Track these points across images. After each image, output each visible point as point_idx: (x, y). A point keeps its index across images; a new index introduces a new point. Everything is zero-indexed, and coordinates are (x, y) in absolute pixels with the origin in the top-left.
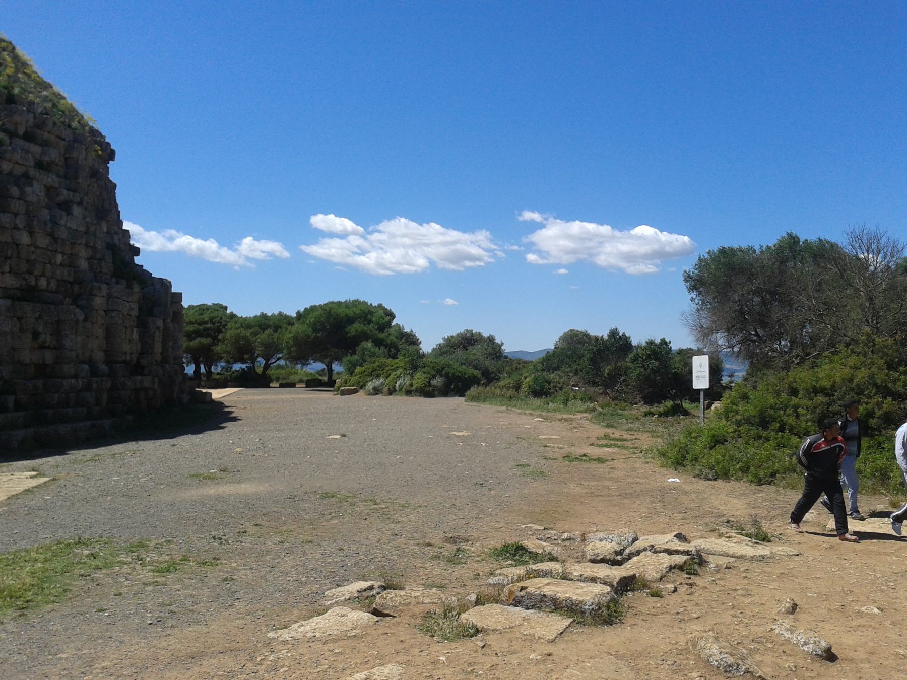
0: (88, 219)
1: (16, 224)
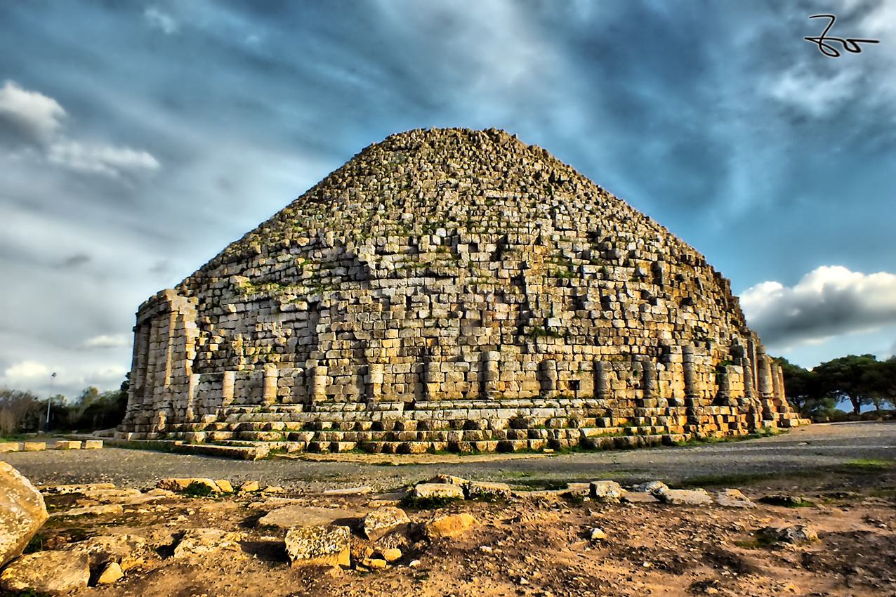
0: (668, 307)
1: (614, 317)
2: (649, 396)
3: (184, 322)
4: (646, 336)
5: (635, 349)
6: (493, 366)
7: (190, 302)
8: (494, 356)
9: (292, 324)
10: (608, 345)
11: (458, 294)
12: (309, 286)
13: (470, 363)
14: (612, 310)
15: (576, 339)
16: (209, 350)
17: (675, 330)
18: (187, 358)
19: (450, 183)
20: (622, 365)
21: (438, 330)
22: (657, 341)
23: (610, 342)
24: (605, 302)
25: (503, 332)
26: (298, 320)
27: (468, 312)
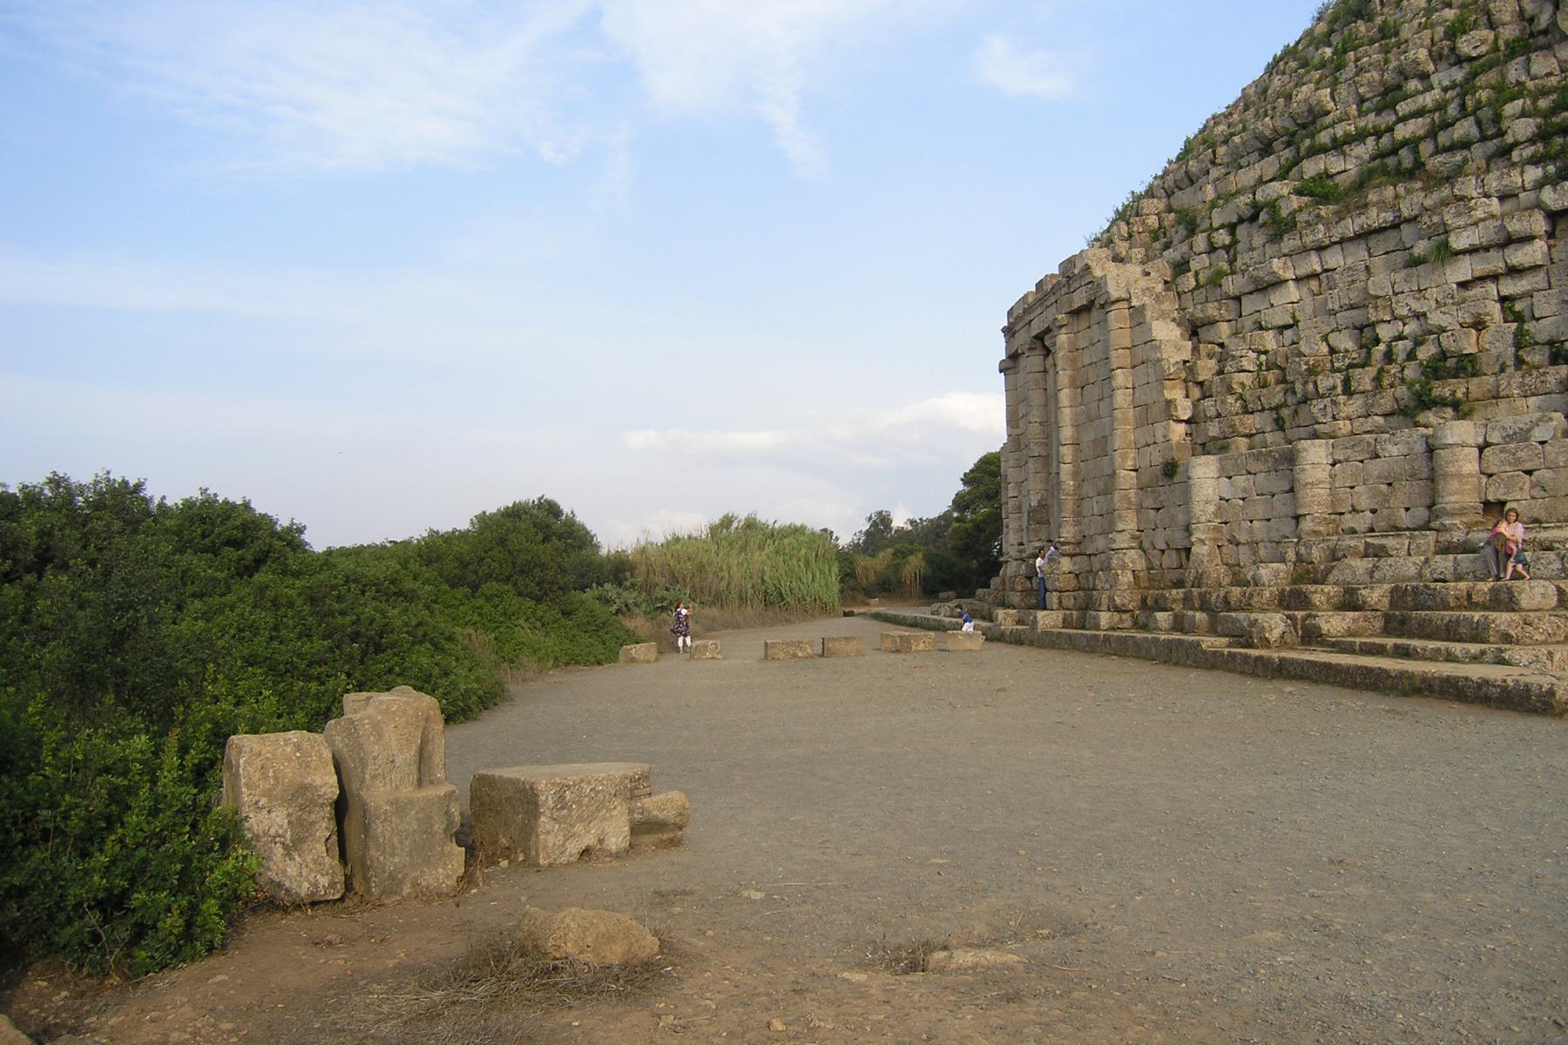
7: (1148, 274)
12: (1535, 161)
16: (1230, 390)
18: (1170, 417)
26: (1514, 271)
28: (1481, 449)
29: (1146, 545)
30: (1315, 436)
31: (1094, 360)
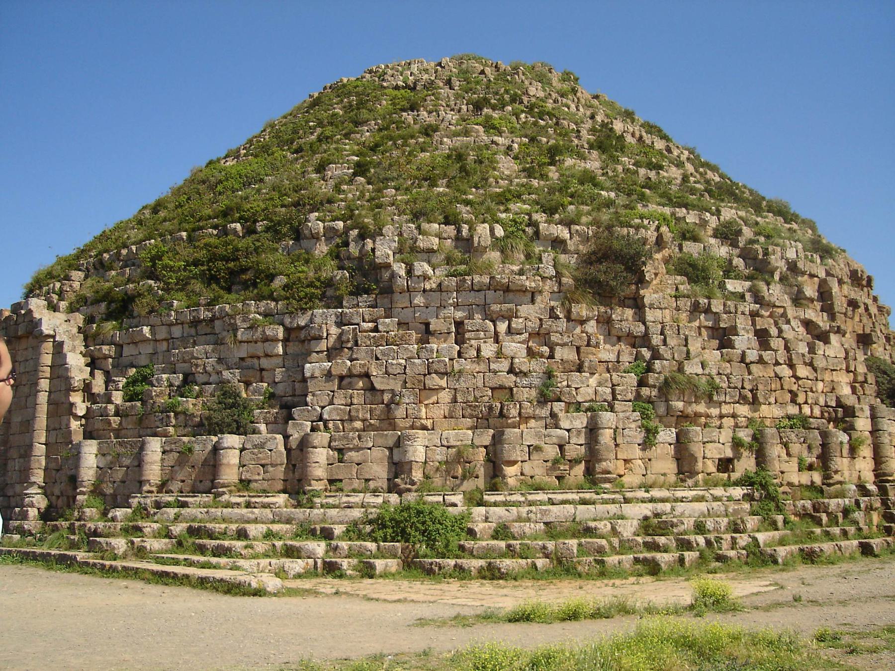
1: (776, 360)
2: (831, 481)
3: (66, 355)
4: (820, 391)
5: (806, 410)
6: (606, 436)
8: (607, 418)
9: (255, 361)
10: (769, 404)
11: (541, 320)
13: (568, 431)
14: (773, 350)
15: (726, 394)
16: (110, 401)
17: (855, 381)
19: (497, 144)
20: (793, 435)
21: (512, 377)
22: (834, 398)
23: (772, 400)
24: (762, 337)
25: (615, 382)
27: (558, 348)
28: (241, 452)
29: (49, 492)
30: (155, 435)
31: (27, 370)
